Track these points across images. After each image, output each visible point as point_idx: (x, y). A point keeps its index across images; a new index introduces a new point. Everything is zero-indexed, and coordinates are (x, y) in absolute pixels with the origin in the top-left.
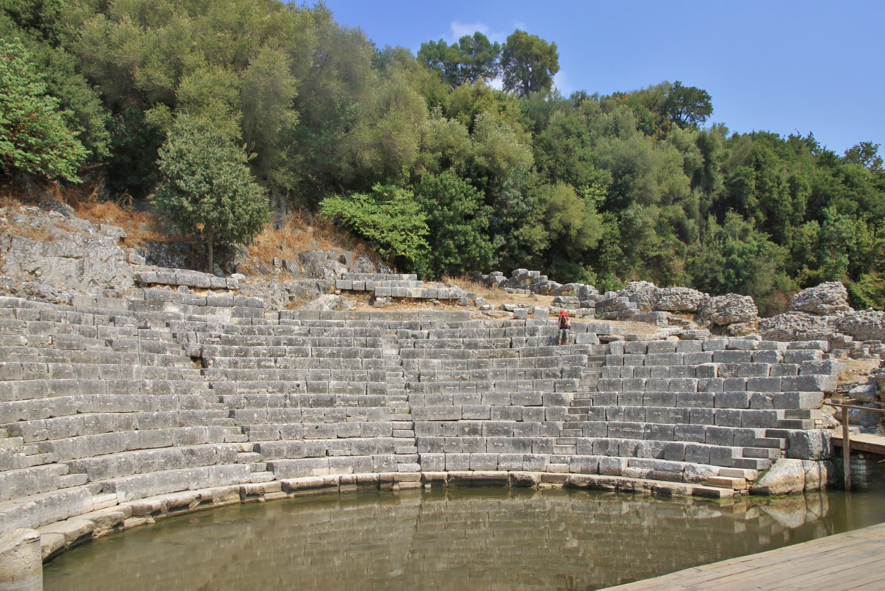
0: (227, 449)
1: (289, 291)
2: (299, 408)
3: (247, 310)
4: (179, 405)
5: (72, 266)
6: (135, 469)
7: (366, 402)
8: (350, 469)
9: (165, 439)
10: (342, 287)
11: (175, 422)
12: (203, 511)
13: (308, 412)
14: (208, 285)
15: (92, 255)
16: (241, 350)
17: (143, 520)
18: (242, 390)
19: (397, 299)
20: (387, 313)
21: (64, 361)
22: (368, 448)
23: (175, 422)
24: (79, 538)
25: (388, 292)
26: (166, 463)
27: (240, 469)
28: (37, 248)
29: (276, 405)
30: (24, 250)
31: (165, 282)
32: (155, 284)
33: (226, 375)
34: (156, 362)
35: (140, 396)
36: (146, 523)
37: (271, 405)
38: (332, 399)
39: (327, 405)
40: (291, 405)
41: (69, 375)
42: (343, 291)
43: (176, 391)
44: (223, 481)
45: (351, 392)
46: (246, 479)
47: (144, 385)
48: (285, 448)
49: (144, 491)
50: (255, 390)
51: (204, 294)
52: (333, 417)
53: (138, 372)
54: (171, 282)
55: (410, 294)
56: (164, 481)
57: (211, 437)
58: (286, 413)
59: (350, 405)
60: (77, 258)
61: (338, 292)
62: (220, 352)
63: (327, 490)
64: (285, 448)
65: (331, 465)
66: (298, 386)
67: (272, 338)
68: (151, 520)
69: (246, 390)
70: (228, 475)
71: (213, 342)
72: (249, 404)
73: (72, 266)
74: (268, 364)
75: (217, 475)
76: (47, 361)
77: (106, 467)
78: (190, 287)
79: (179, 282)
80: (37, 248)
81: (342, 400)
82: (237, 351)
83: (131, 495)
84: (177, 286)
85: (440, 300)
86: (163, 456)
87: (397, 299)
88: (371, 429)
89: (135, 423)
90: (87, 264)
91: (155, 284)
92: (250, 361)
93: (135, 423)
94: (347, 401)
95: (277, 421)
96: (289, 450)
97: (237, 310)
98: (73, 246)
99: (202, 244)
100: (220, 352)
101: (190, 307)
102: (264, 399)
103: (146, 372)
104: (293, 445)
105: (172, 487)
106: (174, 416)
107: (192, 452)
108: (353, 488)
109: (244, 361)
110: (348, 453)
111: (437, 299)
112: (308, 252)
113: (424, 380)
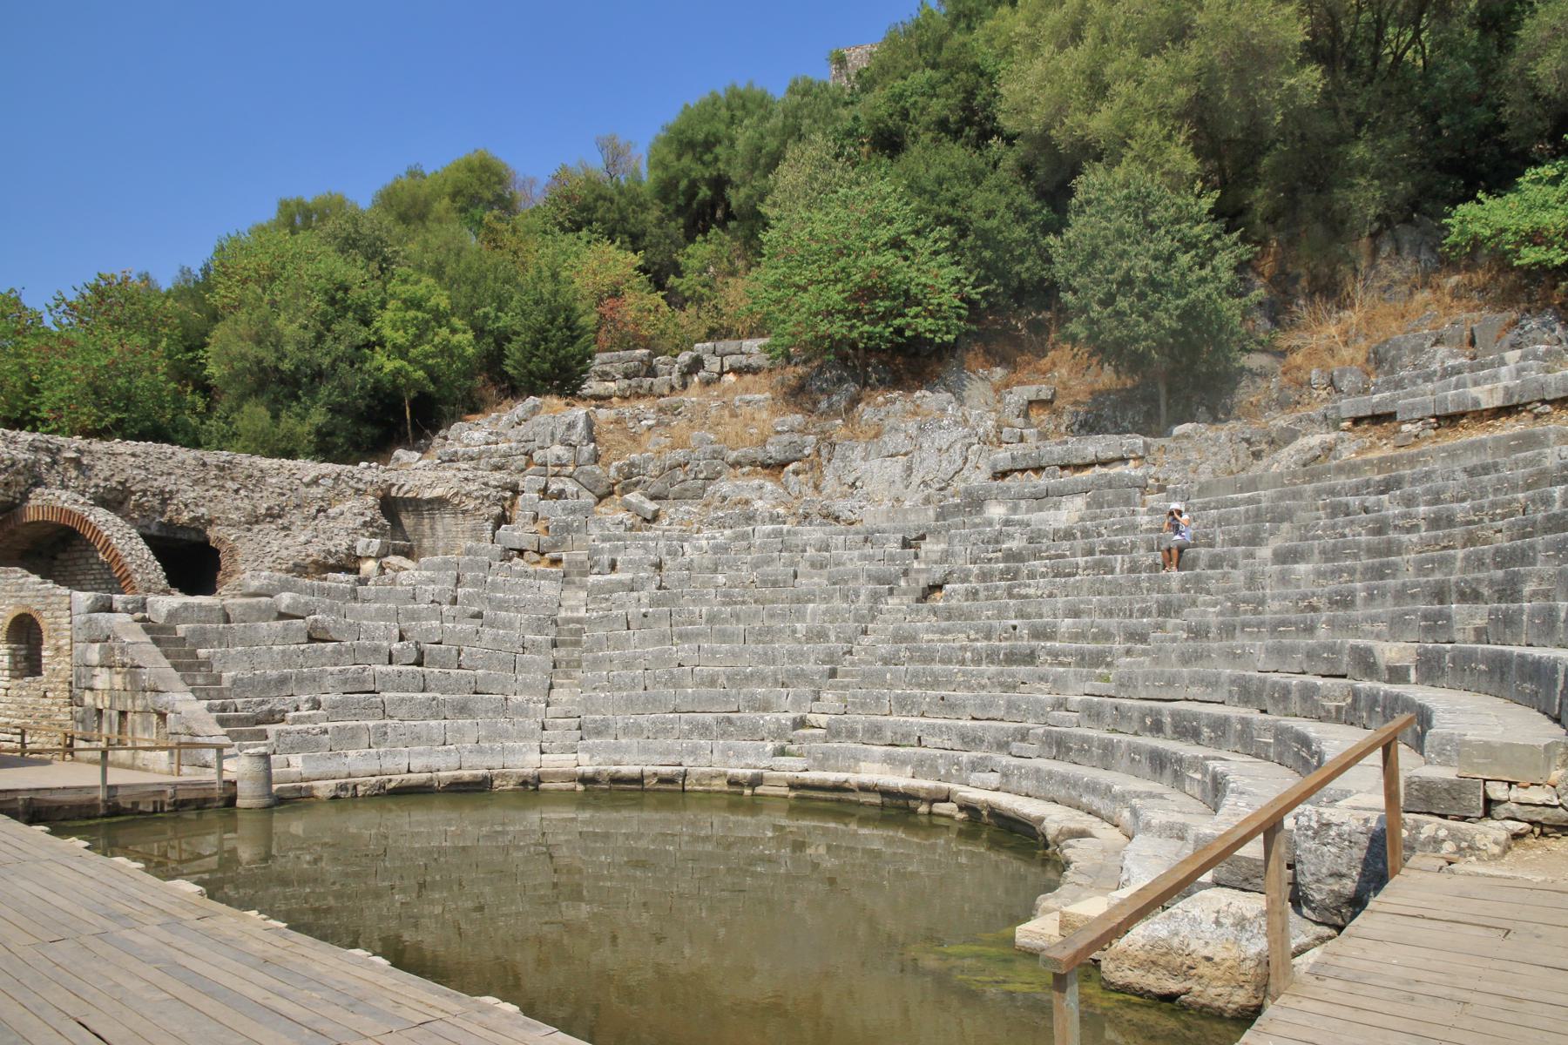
0: (778, 720)
1: (1248, 441)
2: (983, 667)
3: (1109, 495)
4: (812, 659)
5: (896, 467)
6: (646, 733)
7: (1083, 659)
8: (909, 770)
9: (727, 703)
10: (1353, 414)
11: (776, 680)
12: (670, 791)
13: (964, 674)
14: (1090, 458)
15: (925, 445)
16: (1008, 571)
17: (571, 785)
18: (931, 636)
19: (1450, 420)
20: (1366, 462)
21: (744, 602)
22: (973, 740)
23: (776, 681)
24: (451, 784)
25: (1425, 408)
26: (691, 731)
27: (756, 748)
28: (859, 451)
29: (950, 662)
30: (844, 458)
31: (1024, 465)
32: (1012, 471)
33: (935, 614)
34: (862, 598)
35: (790, 645)
36: (574, 790)
37: (942, 661)
38: (1033, 652)
39: (1026, 663)
40: (973, 661)
41: (726, 621)
42: (1357, 421)
43: (838, 638)
44: (733, 762)
45: (1095, 638)
46: (765, 763)
47: (794, 631)
48: (860, 727)
49: (617, 758)
50: (950, 637)
51: (1087, 474)
52: (1001, 684)
53: (814, 613)
54: (1031, 464)
55: (1476, 402)
56: (645, 750)
57: (792, 703)
58: (932, 673)
59: (1061, 664)
60: (906, 454)
61: (1347, 424)
62: (977, 576)
63: (844, 796)
64: (860, 727)
65: (889, 760)
66: (1015, 628)
67: (1080, 543)
68: (580, 787)
69: (936, 637)
70: (739, 754)
71: (990, 560)
72: (911, 659)
73: (896, 467)
74: (1023, 592)
75: (724, 752)
76: (724, 604)
77: (607, 727)
78: (1063, 467)
79: (1043, 463)
80: (859, 451)
81: (1049, 654)
82: (1002, 572)
83: (598, 759)
84: (1043, 468)
85: (1551, 402)
86: (688, 722)
87: (1450, 420)
88: (1018, 708)
89: (722, 680)
90: (916, 460)
91: (1012, 471)
92: (997, 588)
93: (722, 680)
94: (1055, 654)
95: (920, 686)
96: (866, 731)
97: (1093, 498)
98: (893, 441)
99: (1177, 379)
100: (977, 576)
101: (1023, 503)
102: (932, 651)
103: (824, 614)
104: (871, 723)
105: (657, 759)
106: (775, 674)
107: (729, 721)
108: (877, 799)
109: (987, 589)
110: (948, 744)
111: (1544, 402)
112: (1386, 342)
113: (1245, 612)
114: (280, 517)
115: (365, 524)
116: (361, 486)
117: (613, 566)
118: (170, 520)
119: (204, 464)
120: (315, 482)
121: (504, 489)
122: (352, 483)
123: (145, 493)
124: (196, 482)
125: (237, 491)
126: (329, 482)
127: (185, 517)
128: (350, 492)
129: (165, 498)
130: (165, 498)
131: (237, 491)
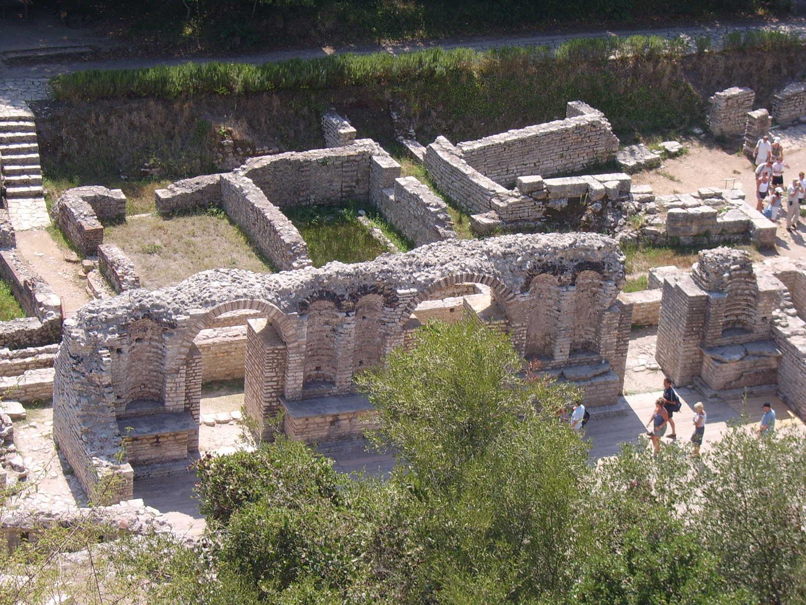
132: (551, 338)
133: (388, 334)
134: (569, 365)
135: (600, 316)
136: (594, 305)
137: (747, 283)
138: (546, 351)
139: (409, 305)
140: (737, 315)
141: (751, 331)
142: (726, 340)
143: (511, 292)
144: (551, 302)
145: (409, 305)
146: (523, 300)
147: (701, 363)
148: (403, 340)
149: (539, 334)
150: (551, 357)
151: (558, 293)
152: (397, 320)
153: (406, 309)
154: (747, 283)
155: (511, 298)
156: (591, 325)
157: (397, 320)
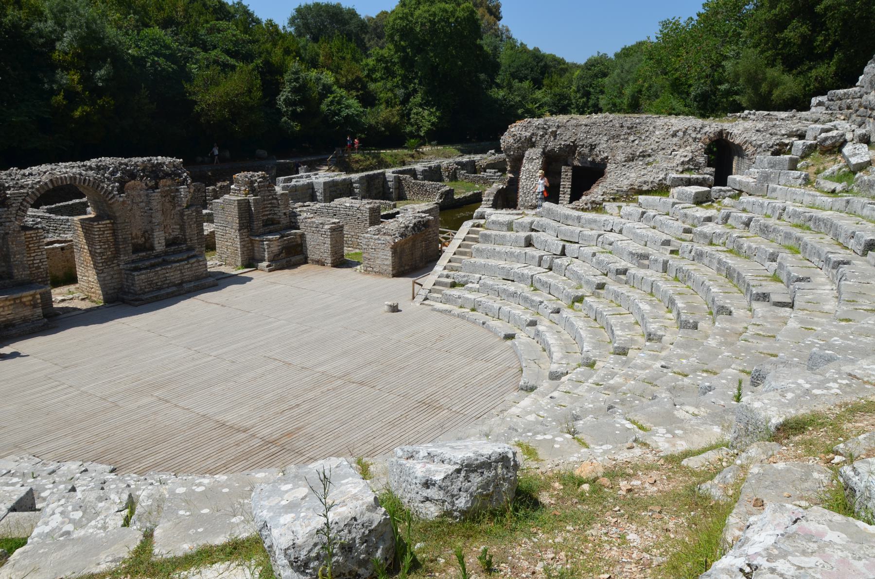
114: (649, 156)
115: (683, 163)
116: (699, 136)
117: (726, 218)
118: (594, 160)
119: (622, 126)
120: (674, 135)
121: (790, 135)
122: (693, 135)
123: (583, 146)
124: (613, 137)
125: (633, 141)
126: (680, 134)
127: (598, 159)
128: (691, 140)
129: (592, 147)
130: (592, 147)
131: (633, 141)
132: (148, 234)
133: (8, 233)
134: (166, 253)
135: (182, 214)
136: (174, 207)
137: (269, 191)
138: (147, 245)
139: (22, 204)
140: (267, 215)
141: (279, 223)
142: (267, 229)
143: (110, 193)
144: (144, 204)
145: (22, 204)
146: (121, 199)
147: (253, 249)
148: (23, 238)
149: (139, 233)
150: (152, 248)
151: (147, 195)
152: (13, 219)
153: (20, 209)
154: (269, 191)
155: (112, 198)
156: (176, 224)
157: (13, 219)
